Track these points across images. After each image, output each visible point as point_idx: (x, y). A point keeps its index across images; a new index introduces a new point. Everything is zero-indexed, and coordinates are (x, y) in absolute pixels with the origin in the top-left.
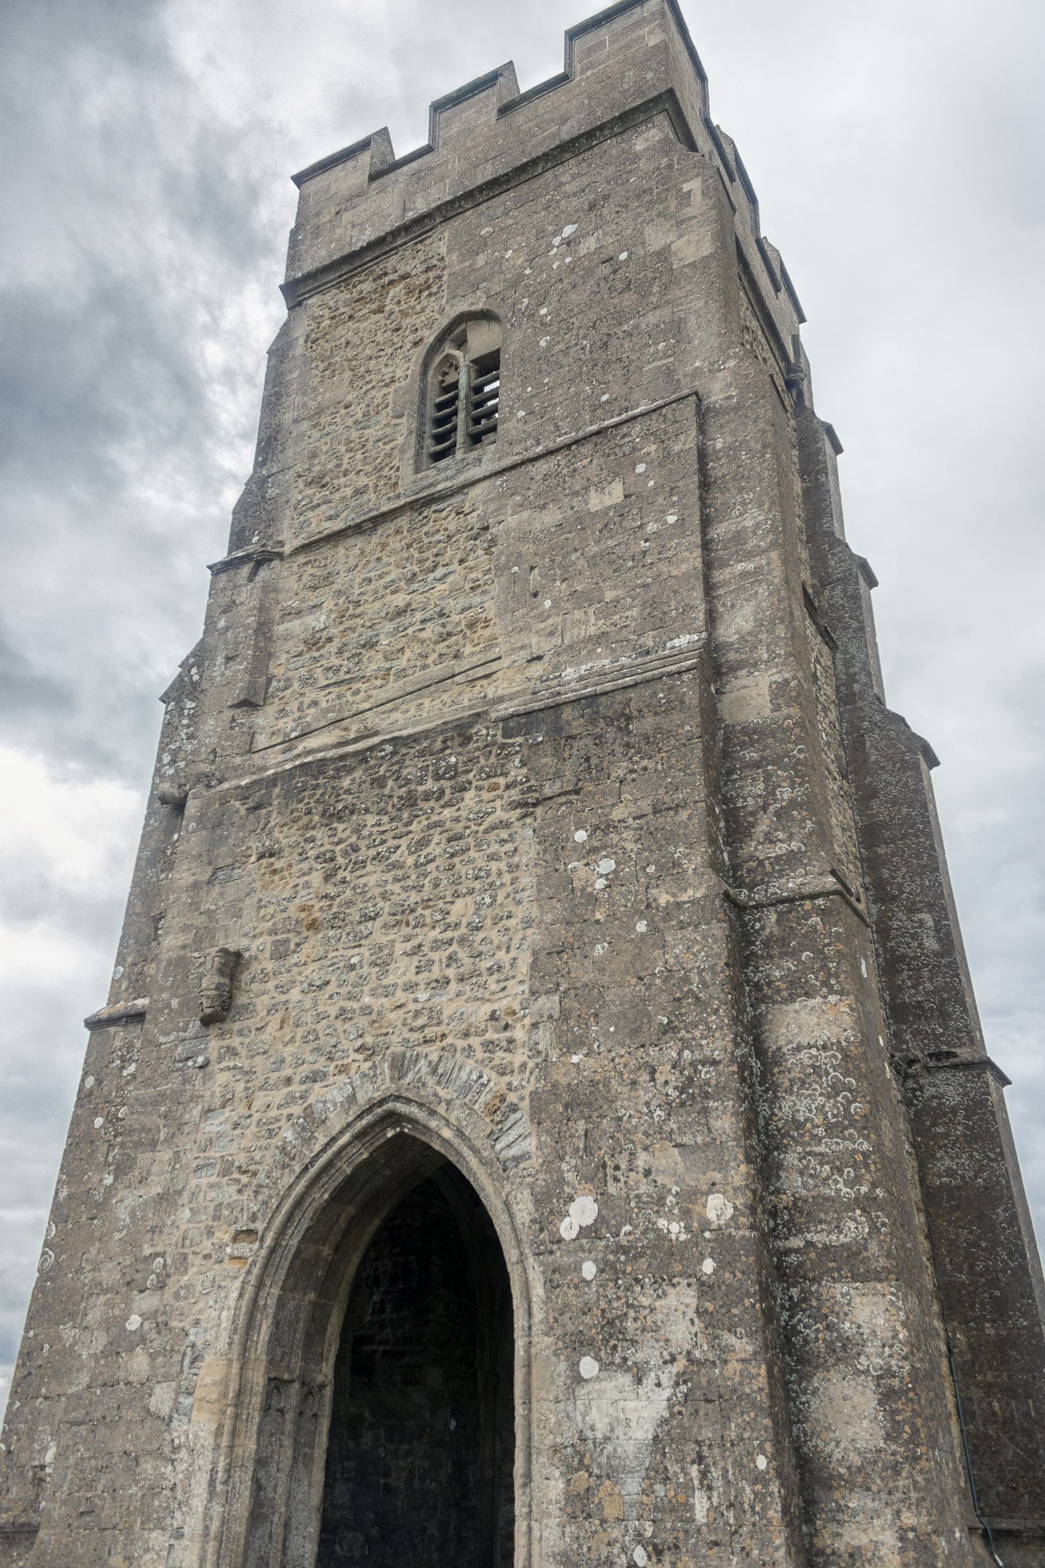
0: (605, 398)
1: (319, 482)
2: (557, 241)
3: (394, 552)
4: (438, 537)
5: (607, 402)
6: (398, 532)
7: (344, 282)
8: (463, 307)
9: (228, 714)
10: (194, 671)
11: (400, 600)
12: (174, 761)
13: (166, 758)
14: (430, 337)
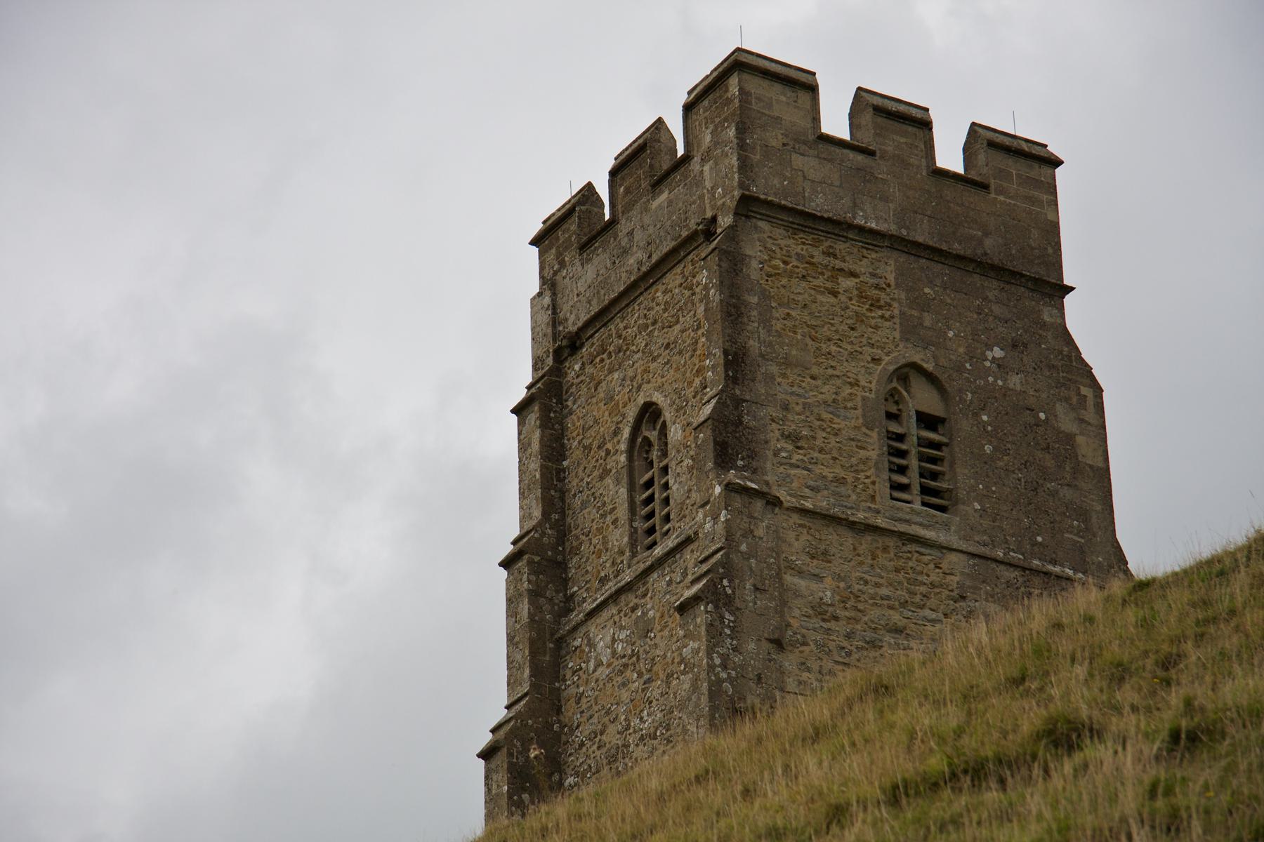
0: (1039, 539)
1: (793, 438)
2: (989, 355)
3: (883, 568)
4: (923, 578)
5: (1040, 544)
6: (885, 549)
7: (793, 230)
8: (917, 357)
9: (766, 646)
10: (725, 582)
11: (896, 618)
12: (724, 666)
13: (718, 661)
14: (889, 363)
